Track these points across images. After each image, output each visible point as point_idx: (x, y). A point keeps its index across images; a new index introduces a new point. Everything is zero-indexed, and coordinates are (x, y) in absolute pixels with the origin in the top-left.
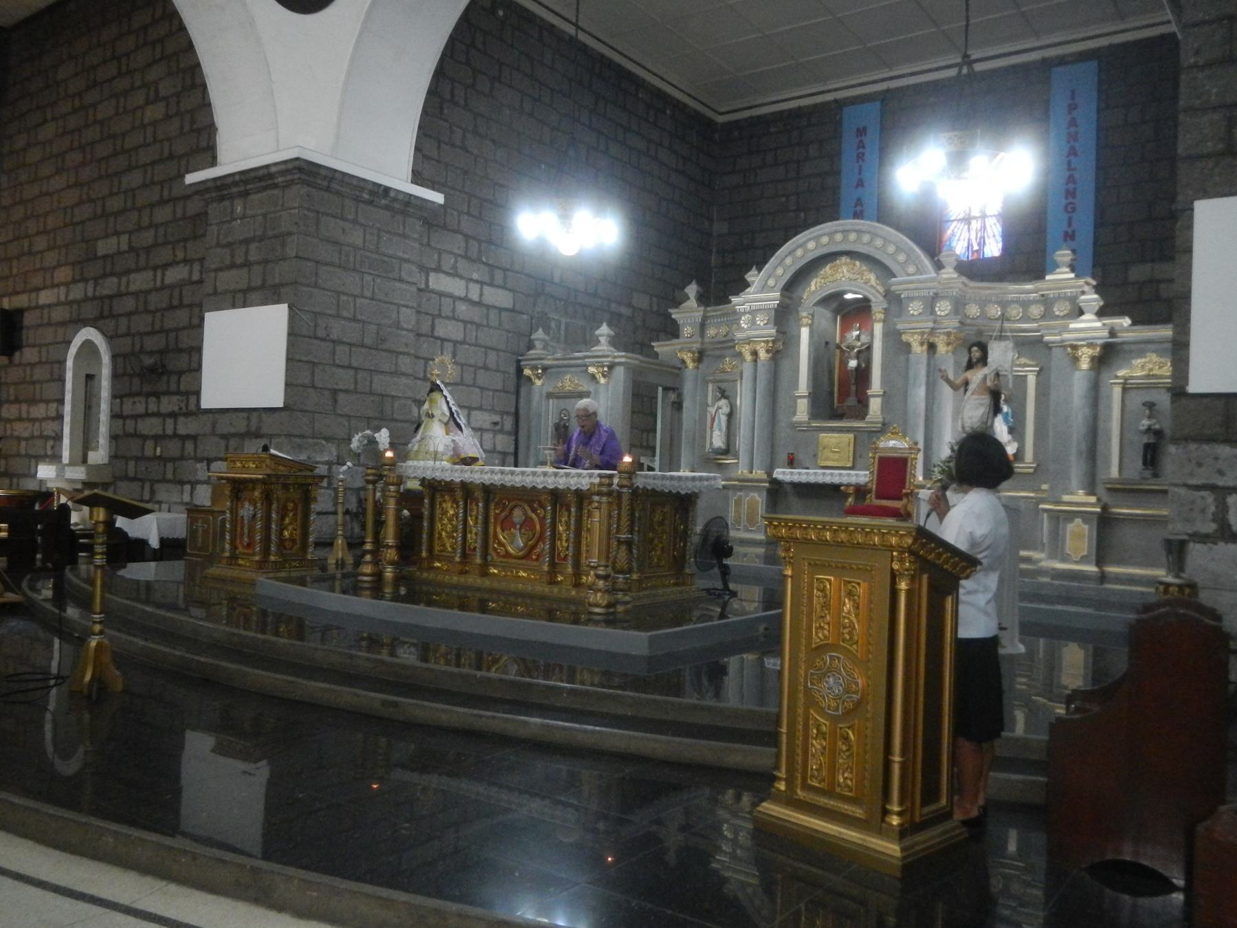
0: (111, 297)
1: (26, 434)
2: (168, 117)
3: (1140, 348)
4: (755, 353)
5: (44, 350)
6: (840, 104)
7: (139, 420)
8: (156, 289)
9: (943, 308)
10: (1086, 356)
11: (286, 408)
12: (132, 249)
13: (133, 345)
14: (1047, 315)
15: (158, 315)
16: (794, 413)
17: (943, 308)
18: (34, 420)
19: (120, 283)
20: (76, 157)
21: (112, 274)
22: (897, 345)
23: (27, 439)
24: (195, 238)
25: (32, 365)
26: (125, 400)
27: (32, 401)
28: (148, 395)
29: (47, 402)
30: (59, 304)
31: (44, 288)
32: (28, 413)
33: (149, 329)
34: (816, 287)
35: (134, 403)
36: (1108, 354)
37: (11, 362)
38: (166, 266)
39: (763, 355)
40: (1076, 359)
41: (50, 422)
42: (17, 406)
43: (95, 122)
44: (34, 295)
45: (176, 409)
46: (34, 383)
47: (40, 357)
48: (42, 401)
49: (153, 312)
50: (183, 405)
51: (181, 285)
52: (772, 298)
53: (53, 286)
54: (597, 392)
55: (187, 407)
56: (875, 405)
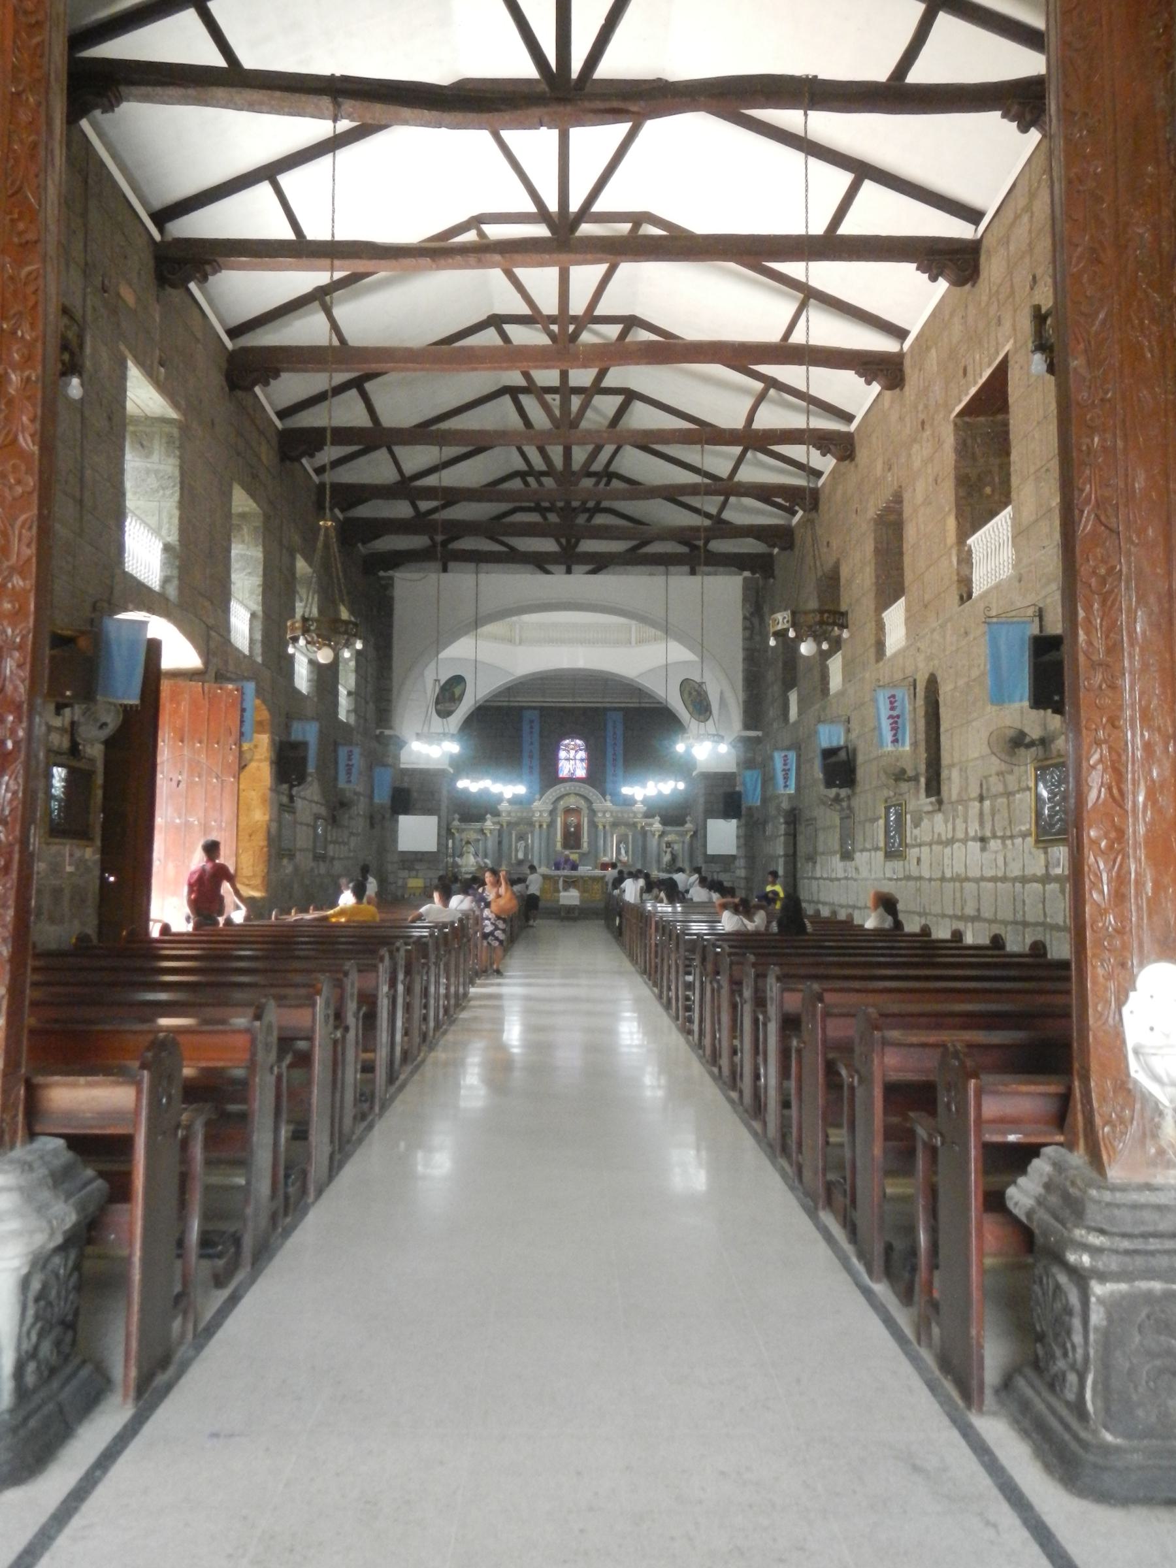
3: (670, 833)
4: (541, 826)
6: (522, 709)
9: (608, 815)
10: (657, 834)
11: (439, 851)
14: (635, 817)
16: (555, 845)
17: (608, 815)
22: (593, 825)
34: (562, 804)
36: (663, 834)
39: (545, 826)
40: (654, 835)
52: (550, 807)
54: (486, 839)
56: (585, 845)
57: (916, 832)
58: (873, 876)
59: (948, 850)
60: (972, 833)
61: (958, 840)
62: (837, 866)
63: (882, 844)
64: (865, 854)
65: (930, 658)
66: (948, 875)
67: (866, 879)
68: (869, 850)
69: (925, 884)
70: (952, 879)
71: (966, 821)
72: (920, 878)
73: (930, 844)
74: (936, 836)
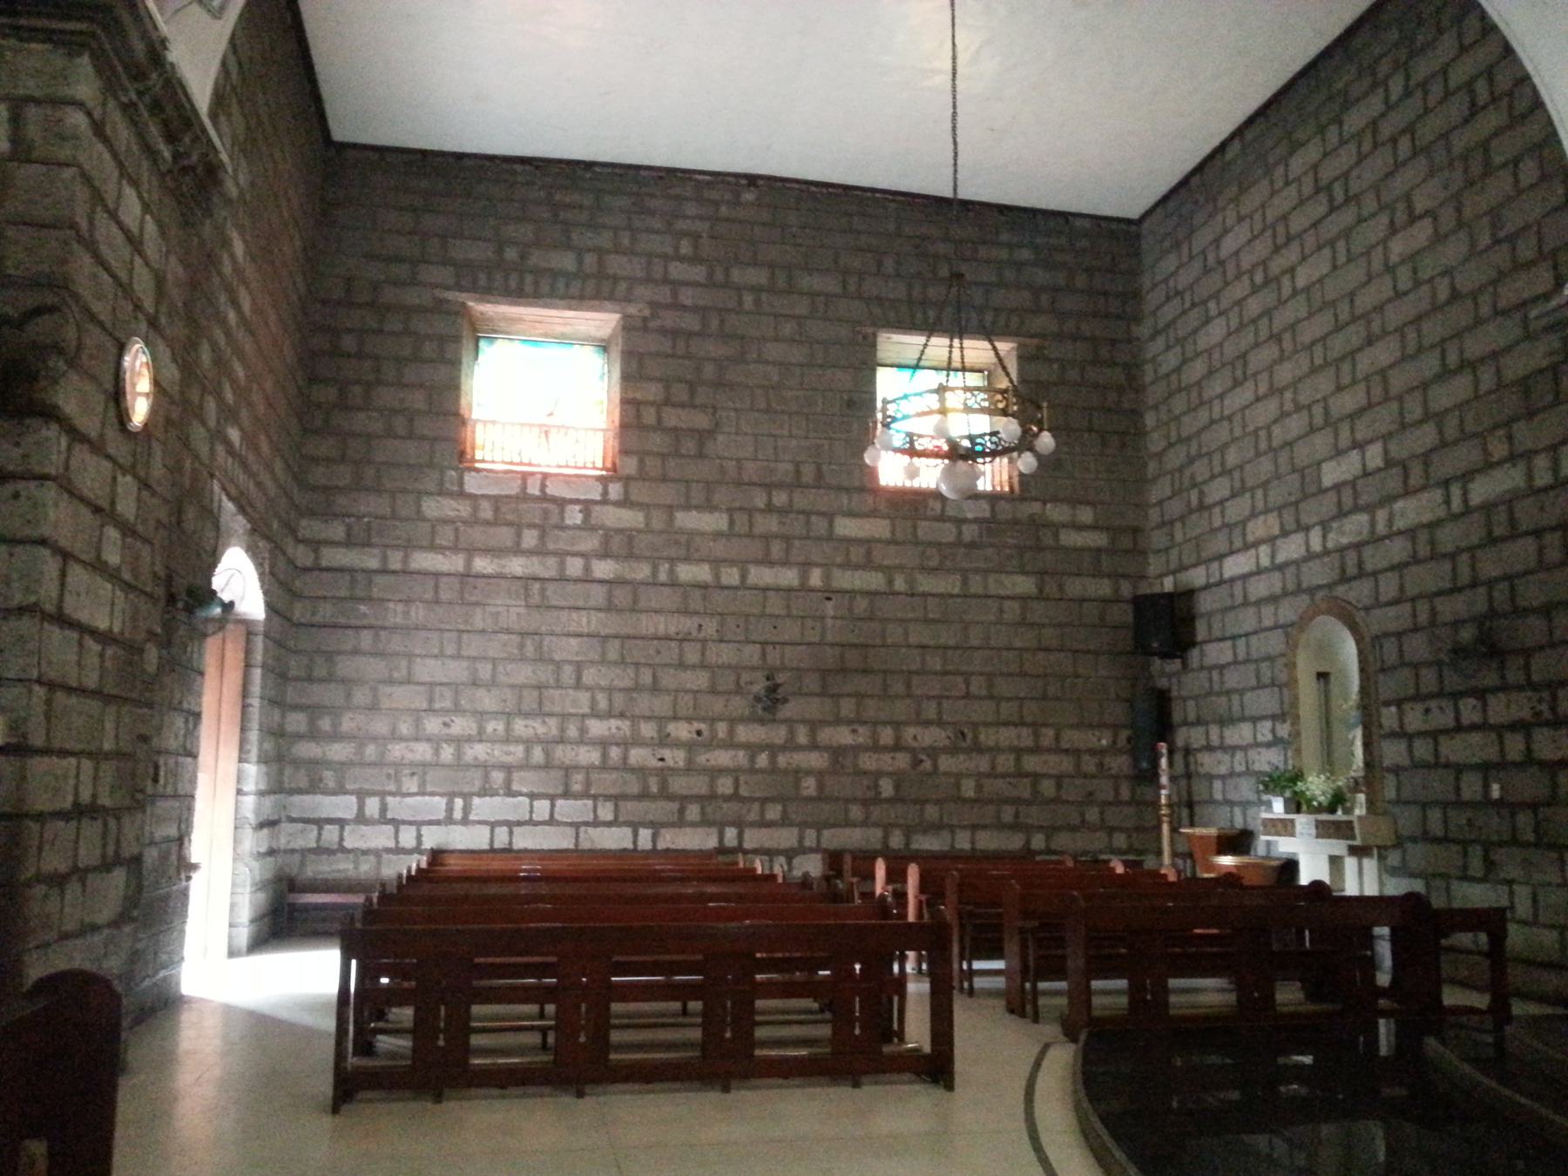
0: (1358, 546)
1: (1223, 770)
2: (1438, 238)
5: (1241, 643)
7: (1442, 739)
8: (1455, 517)
12: (1389, 463)
13: (1415, 616)
15: (1464, 558)
18: (1233, 749)
19: (1373, 524)
20: (1268, 353)
21: (1357, 509)
23: (1223, 777)
24: (1531, 414)
25: (1222, 668)
26: (1407, 707)
27: (1225, 721)
28: (1456, 696)
29: (1255, 720)
30: (1259, 571)
31: (1232, 553)
32: (1222, 737)
33: (1448, 585)
35: (1427, 711)
37: (1185, 665)
38: (1466, 477)
41: (1263, 750)
42: (1201, 729)
43: (1295, 293)
44: (1215, 565)
45: (1526, 714)
46: (1228, 692)
47: (1235, 654)
48: (1243, 719)
49: (1452, 557)
50: (1544, 707)
51: (1510, 500)
53: (1247, 547)
55: (1553, 709)
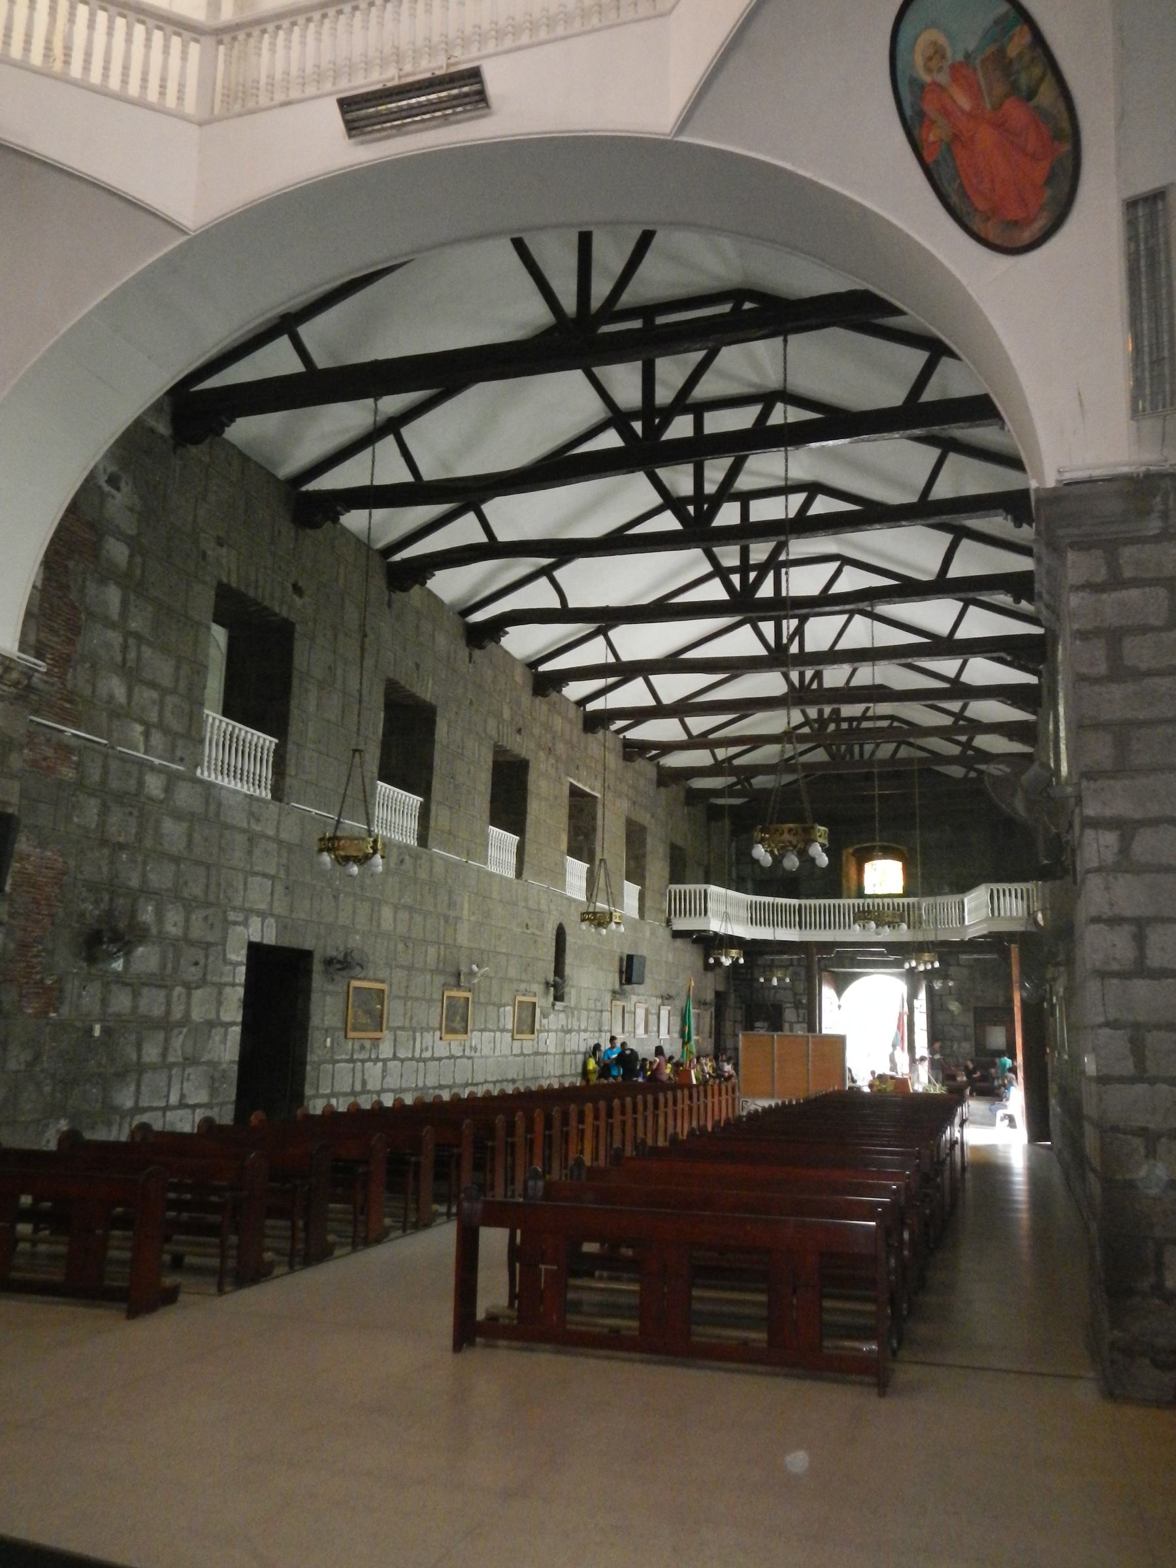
57: (545, 1021)
58: (496, 1054)
59: (568, 1036)
60: (583, 1027)
61: (575, 1031)
62: (443, 1045)
63: (510, 1027)
64: (486, 1034)
65: (561, 914)
66: (568, 1050)
67: (487, 1057)
68: (494, 1031)
69: (551, 1058)
70: (570, 1053)
71: (579, 1020)
72: (547, 1053)
73: (556, 1031)
74: (560, 1027)
